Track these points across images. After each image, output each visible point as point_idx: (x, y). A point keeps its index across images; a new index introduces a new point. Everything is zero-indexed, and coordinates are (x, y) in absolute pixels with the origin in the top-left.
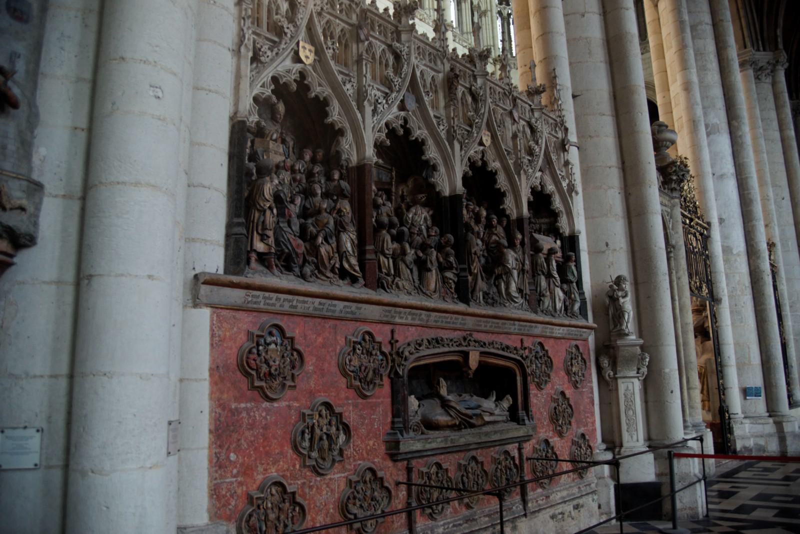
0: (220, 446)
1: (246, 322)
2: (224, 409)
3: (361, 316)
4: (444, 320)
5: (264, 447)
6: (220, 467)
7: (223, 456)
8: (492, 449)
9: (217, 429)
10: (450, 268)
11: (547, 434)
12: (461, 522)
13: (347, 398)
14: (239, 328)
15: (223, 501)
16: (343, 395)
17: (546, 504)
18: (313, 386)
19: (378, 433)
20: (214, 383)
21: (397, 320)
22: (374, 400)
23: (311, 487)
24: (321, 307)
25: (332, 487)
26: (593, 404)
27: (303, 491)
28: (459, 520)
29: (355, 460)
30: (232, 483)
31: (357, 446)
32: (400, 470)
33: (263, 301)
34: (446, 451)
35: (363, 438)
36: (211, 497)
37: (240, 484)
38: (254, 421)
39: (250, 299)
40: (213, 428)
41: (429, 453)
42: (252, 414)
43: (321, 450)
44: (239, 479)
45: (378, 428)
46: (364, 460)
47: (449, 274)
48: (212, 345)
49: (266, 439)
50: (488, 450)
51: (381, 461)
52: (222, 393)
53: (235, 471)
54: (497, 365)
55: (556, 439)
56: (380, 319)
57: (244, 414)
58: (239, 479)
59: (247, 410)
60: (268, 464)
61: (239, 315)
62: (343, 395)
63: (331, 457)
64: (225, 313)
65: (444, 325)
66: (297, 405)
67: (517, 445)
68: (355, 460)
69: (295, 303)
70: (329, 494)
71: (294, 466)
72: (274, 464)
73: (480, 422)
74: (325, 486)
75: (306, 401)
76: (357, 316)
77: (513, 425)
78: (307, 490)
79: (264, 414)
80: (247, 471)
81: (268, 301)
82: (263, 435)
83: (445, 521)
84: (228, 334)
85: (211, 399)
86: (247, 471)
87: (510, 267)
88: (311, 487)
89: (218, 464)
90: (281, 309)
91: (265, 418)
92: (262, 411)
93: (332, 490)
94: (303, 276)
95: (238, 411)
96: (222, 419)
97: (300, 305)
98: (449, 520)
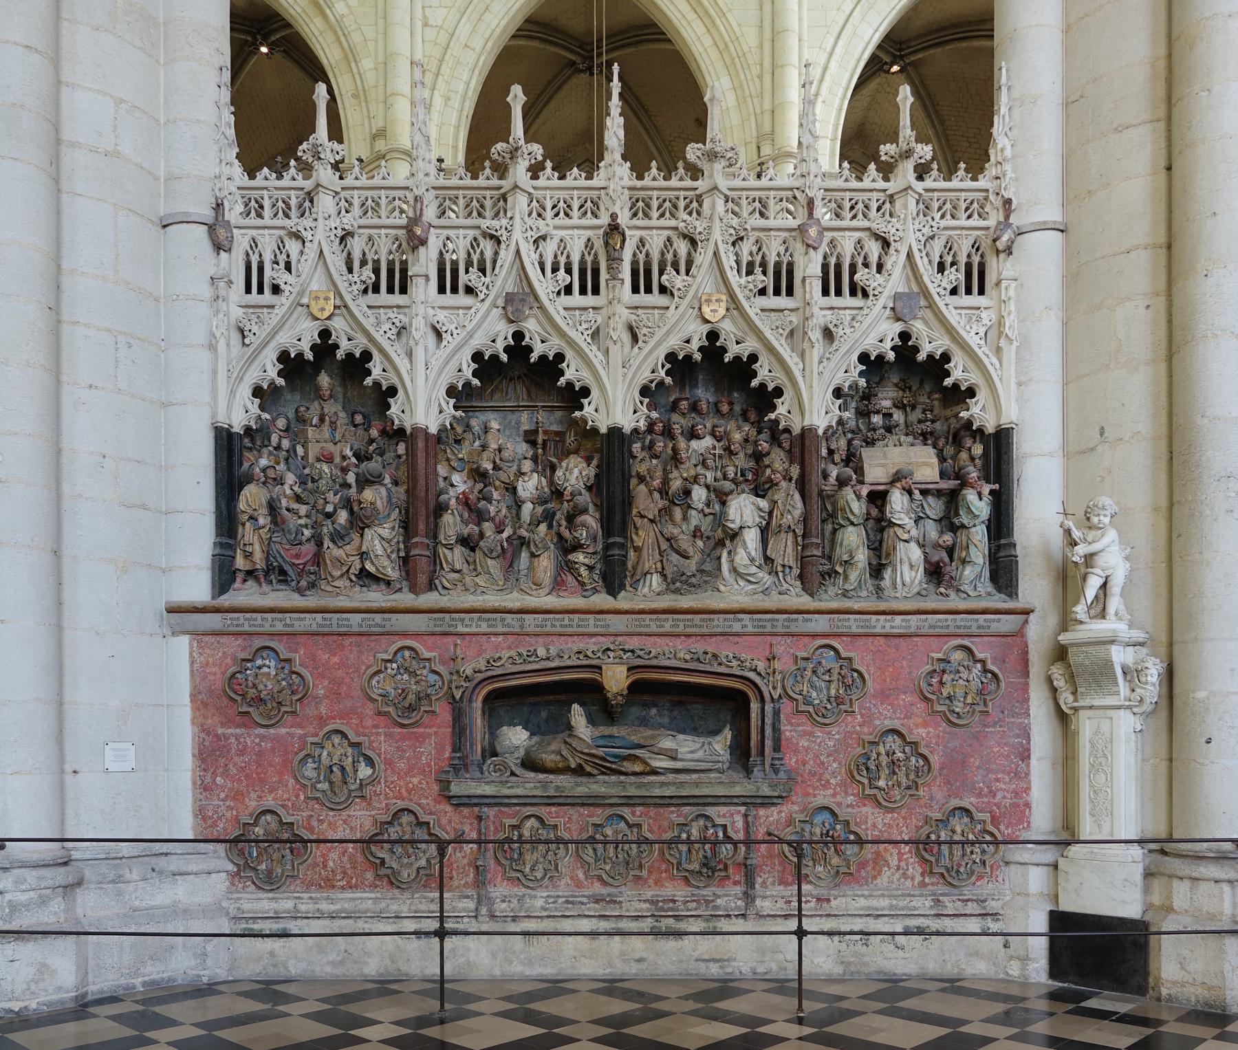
0: (205, 770)
1: (234, 647)
2: (208, 734)
3: (394, 629)
4: (557, 624)
5: (258, 774)
6: (205, 790)
7: (208, 780)
8: (673, 809)
9: (200, 753)
10: (577, 547)
11: (839, 798)
12: (585, 900)
13: (376, 727)
14: (224, 653)
15: (209, 822)
16: (369, 723)
17: (816, 909)
18: (324, 712)
19: (427, 769)
20: (195, 709)
21: (460, 629)
22: (422, 730)
23: (319, 821)
24: (328, 623)
25: (353, 824)
26: (1025, 755)
27: (309, 823)
28: (584, 896)
29: (387, 798)
30: (219, 806)
31: (392, 782)
32: (465, 817)
33: (246, 624)
34: (550, 801)
35: (402, 773)
36: (196, 816)
37: (230, 808)
38: (245, 746)
39: (229, 622)
40: (196, 752)
41: (514, 801)
42: (242, 740)
43: (331, 783)
44: (228, 803)
45: (429, 765)
46: (403, 800)
47: (580, 557)
48: (192, 671)
49: (259, 765)
50: (661, 810)
51: (432, 804)
52: (205, 717)
53: (222, 795)
54: (689, 682)
55: (867, 809)
56: (429, 629)
57: (233, 740)
58: (228, 803)
59: (237, 737)
60: (263, 791)
61: (224, 639)
62: (369, 723)
63: (346, 791)
64: (207, 639)
65: (558, 629)
66: (301, 732)
67: (743, 809)
68: (387, 798)
69: (288, 621)
70: (348, 831)
71: (297, 796)
72: (271, 792)
73: (638, 768)
74: (341, 822)
75: (315, 728)
76: (388, 628)
77: (738, 776)
78: (315, 823)
79: (257, 740)
80: (238, 796)
81: (252, 623)
82: (257, 762)
83: (552, 894)
84: (211, 660)
85: (193, 724)
86: (238, 796)
87: (732, 526)
88: (321, 822)
89: (204, 787)
90: (273, 629)
91: (259, 745)
92: (252, 737)
93: (351, 828)
94: (300, 591)
95: (226, 737)
96: (207, 744)
97: (296, 623)
98: (560, 894)
